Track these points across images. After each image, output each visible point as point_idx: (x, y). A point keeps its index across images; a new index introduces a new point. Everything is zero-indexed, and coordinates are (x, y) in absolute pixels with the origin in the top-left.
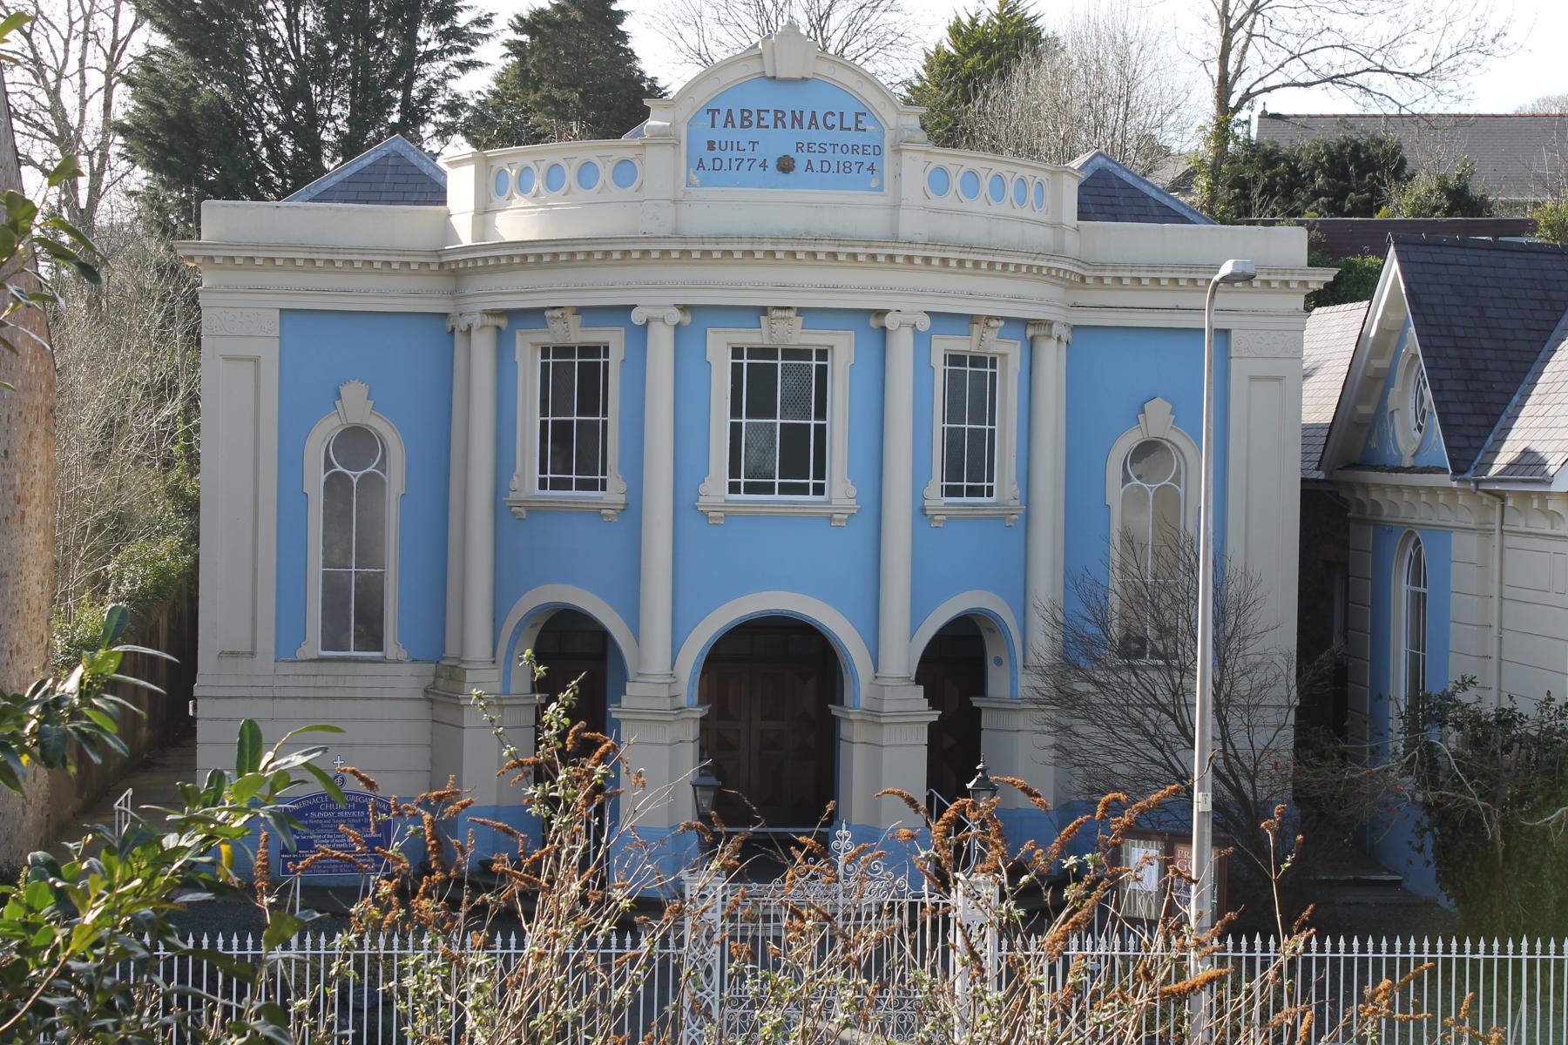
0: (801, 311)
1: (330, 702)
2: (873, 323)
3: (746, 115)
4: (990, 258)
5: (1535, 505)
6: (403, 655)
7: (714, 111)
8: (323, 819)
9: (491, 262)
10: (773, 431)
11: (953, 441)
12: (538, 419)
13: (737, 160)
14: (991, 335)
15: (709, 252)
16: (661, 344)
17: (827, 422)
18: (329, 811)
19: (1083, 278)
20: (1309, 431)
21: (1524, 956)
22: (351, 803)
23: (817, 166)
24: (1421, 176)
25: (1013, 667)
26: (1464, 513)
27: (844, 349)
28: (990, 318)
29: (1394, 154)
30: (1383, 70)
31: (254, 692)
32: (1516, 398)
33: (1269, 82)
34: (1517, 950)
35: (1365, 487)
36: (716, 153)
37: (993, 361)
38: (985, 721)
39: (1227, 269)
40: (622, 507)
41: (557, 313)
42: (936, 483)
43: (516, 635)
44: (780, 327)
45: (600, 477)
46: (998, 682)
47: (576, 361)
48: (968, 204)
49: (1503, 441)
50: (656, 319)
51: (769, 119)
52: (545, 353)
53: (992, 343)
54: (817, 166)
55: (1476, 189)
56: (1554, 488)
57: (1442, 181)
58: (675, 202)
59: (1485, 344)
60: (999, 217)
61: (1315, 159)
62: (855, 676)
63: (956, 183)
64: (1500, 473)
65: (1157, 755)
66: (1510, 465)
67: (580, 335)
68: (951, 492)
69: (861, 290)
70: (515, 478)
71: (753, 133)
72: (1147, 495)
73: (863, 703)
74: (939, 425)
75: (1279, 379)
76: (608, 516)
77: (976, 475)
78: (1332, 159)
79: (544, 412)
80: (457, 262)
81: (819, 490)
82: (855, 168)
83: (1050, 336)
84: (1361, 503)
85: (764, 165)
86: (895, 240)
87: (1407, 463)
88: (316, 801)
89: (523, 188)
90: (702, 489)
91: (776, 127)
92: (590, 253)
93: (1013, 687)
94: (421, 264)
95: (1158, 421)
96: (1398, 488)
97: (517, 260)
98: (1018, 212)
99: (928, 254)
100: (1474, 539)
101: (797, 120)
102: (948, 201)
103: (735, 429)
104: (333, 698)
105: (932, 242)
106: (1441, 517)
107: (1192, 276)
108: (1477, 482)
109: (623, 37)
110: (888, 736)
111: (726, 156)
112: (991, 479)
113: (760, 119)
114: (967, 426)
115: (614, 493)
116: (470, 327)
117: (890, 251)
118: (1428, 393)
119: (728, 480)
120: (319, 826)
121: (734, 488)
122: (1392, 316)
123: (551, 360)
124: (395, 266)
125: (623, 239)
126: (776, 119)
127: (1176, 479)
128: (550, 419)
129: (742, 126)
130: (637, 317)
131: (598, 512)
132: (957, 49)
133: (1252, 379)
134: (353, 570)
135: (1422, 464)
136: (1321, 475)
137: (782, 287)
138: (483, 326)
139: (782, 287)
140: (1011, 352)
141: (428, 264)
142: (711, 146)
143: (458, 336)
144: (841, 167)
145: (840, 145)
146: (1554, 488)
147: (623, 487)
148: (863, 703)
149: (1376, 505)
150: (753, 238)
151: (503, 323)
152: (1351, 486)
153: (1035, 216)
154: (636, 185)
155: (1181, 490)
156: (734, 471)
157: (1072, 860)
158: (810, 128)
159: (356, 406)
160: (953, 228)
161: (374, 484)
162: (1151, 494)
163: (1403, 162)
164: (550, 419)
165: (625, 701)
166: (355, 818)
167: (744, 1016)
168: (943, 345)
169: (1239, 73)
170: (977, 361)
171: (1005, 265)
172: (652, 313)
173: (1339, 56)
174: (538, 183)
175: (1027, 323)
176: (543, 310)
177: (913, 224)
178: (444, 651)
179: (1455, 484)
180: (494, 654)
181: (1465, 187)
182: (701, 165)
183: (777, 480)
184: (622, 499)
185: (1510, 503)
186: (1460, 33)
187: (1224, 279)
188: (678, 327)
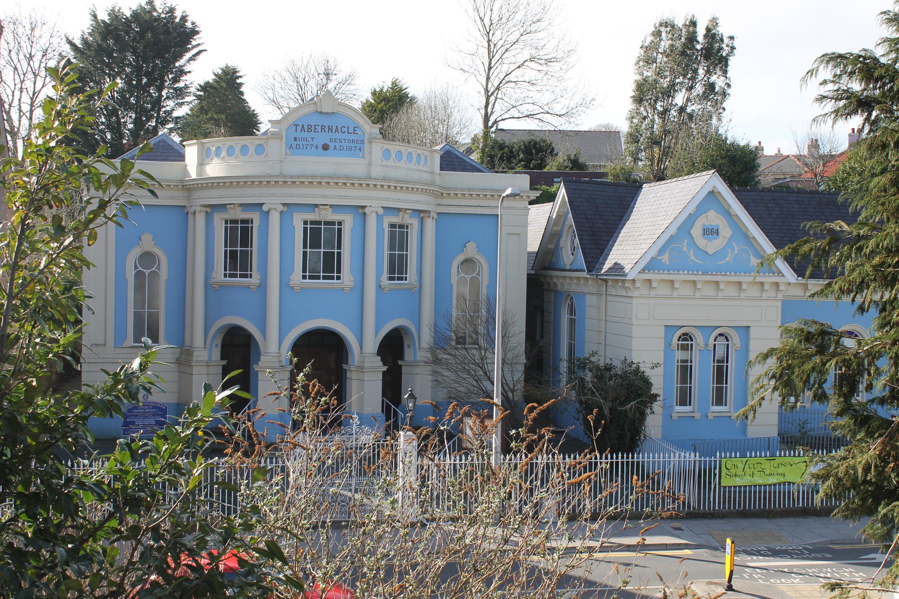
0: (331, 206)
2: (360, 211)
4: (407, 186)
5: (620, 284)
7: (296, 125)
9: (204, 185)
10: (320, 254)
11: (392, 258)
12: (223, 249)
14: (407, 216)
15: (295, 182)
16: (275, 219)
19: (442, 194)
20: (529, 253)
21: (620, 460)
24: (561, 154)
25: (415, 348)
26: (591, 287)
27: (349, 222)
28: (406, 209)
29: (550, 146)
30: (548, 113)
31: (106, 360)
32: (611, 243)
33: (504, 117)
34: (617, 458)
35: (551, 277)
36: (298, 142)
37: (407, 226)
38: (404, 370)
39: (509, 191)
41: (232, 206)
42: (386, 275)
44: (323, 212)
45: (249, 273)
46: (408, 354)
47: (239, 225)
48: (398, 164)
49: (606, 259)
50: (272, 209)
51: (319, 129)
52: (226, 222)
53: (407, 219)
54: (338, 148)
55: (581, 160)
56: (628, 278)
57: (569, 156)
58: (280, 161)
59: (599, 221)
60: (410, 169)
61: (519, 147)
62: (353, 352)
63: (393, 155)
64: (606, 272)
65: (475, 383)
66: (609, 268)
67: (240, 215)
68: (391, 279)
69: (356, 198)
71: (312, 134)
73: (356, 363)
74: (386, 252)
75: (518, 234)
77: (401, 272)
78: (526, 147)
79: (226, 246)
80: (190, 185)
81: (339, 278)
82: (353, 149)
83: (429, 217)
84: (549, 283)
85: (317, 147)
86: (370, 178)
87: (568, 268)
89: (218, 155)
92: (246, 182)
93: (415, 357)
94: (175, 186)
95: (471, 250)
96: (564, 277)
97: (215, 185)
98: (417, 167)
99: (382, 184)
100: (595, 297)
101: (330, 129)
102: (390, 163)
103: (305, 253)
105: (384, 179)
106: (582, 288)
107: (495, 194)
108: (597, 275)
109: (242, 93)
110: (366, 376)
111: (301, 143)
112: (406, 274)
113: (315, 129)
114: (397, 252)
115: (255, 280)
116: (195, 212)
117: (368, 183)
118: (577, 241)
120: (137, 415)
121: (304, 277)
122: (562, 210)
123: (229, 225)
124: (172, 187)
125: (259, 177)
126: (322, 129)
127: (478, 274)
128: (228, 249)
130: (265, 208)
131: (248, 287)
132: (375, 100)
133: (508, 234)
135: (575, 268)
136: (533, 272)
137: (325, 196)
138: (201, 211)
139: (325, 196)
140: (415, 223)
141: (177, 186)
142: (295, 139)
143: (190, 215)
146: (628, 278)
147: (259, 277)
148: (356, 363)
149: (555, 284)
150: (313, 177)
151: (209, 210)
152: (545, 277)
153: (424, 169)
154: (264, 155)
155: (480, 278)
156: (304, 270)
157: (514, 431)
159: (148, 243)
160: (393, 174)
161: (154, 275)
163: (553, 149)
164: (228, 249)
167: (324, 491)
168: (388, 220)
169: (492, 113)
170: (401, 226)
171: (413, 188)
172: (271, 206)
173: (531, 107)
174: (224, 153)
175: (420, 211)
176: (226, 204)
177: (376, 171)
178: (184, 343)
179: (588, 276)
181: (578, 159)
182: (291, 147)
183: (322, 274)
184: (258, 282)
185: (610, 283)
186: (577, 99)
187: (508, 196)
188: (281, 212)
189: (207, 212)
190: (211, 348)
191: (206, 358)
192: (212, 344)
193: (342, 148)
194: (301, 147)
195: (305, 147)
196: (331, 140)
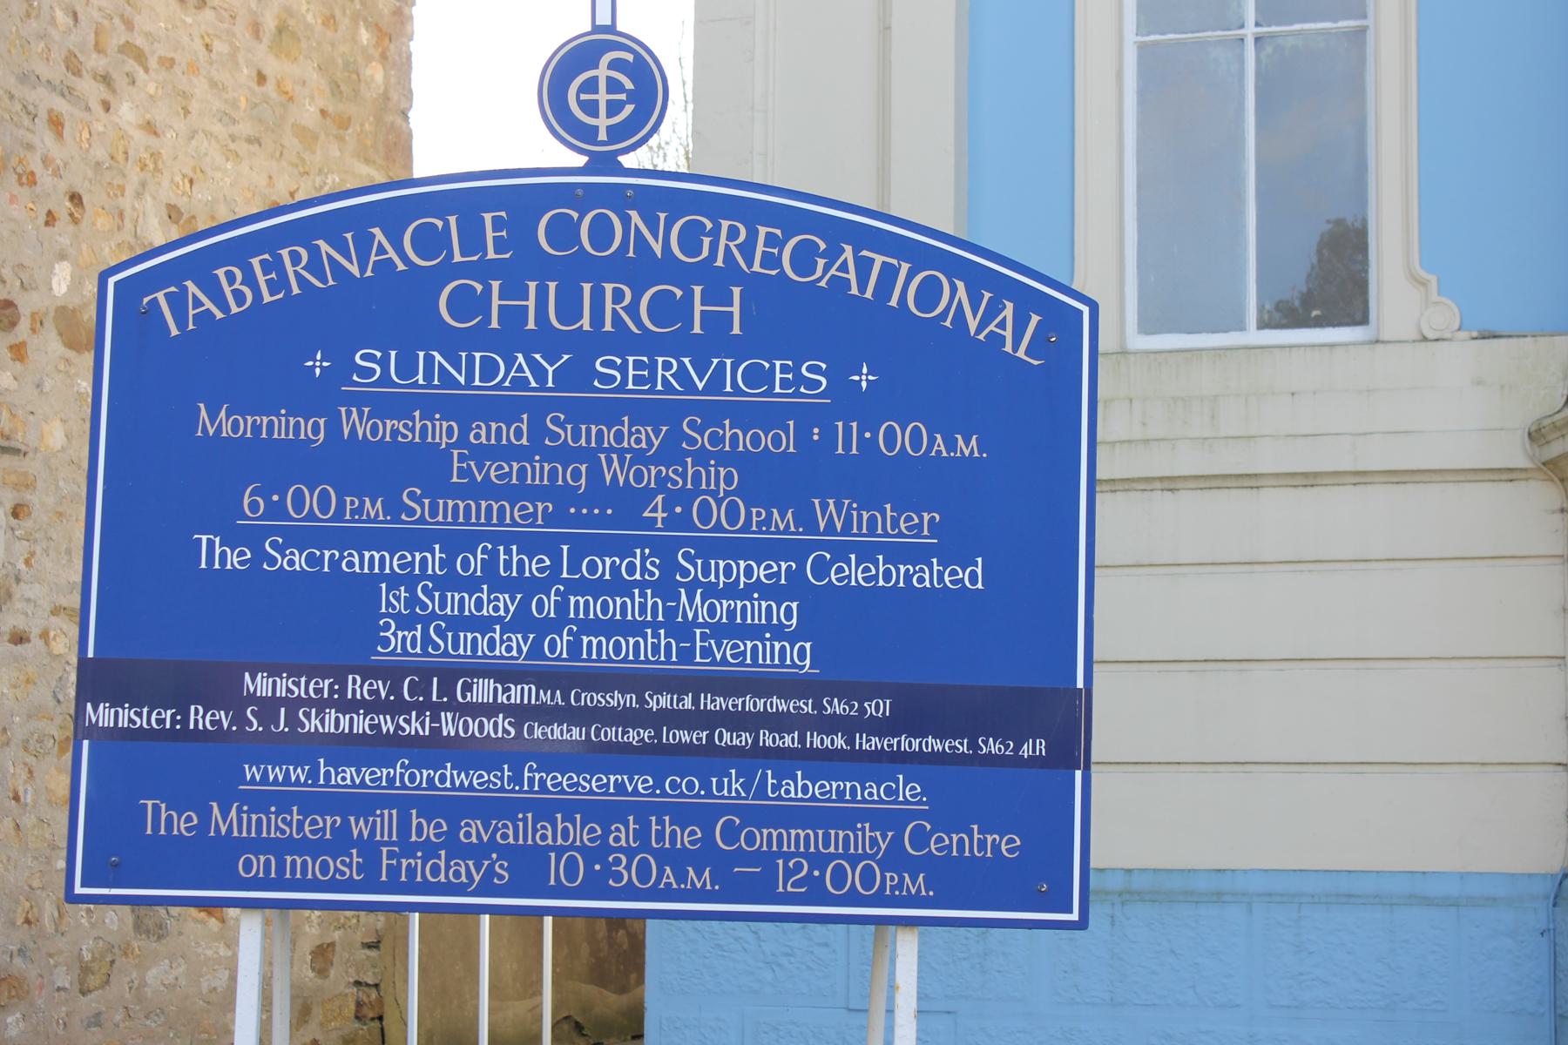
1: (1162, 502)
6: (1444, 317)
8: (466, 410)
18: (512, 337)
22: (717, 282)
88: (405, 254)
104: (1171, 483)
134: (1250, 30)
166: (746, 416)
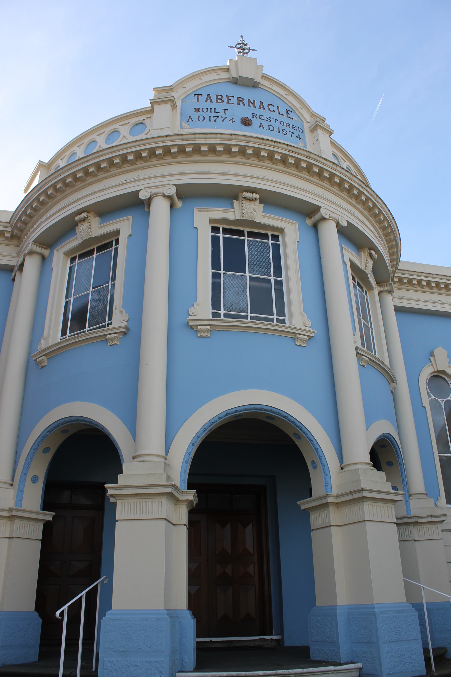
2: (309, 222)
3: (219, 98)
13: (214, 117)
17: (284, 279)
23: (266, 126)
36: (201, 113)
40: (124, 330)
43: (31, 457)
51: (235, 100)
54: (266, 126)
70: (43, 341)
71: (225, 105)
72: (440, 405)
76: (111, 339)
85: (232, 120)
90: (191, 311)
91: (239, 104)
93: (408, 508)
101: (252, 103)
111: (207, 115)
113: (228, 100)
119: (211, 311)
126: (239, 101)
129: (217, 102)
142: (197, 110)
144: (281, 131)
145: (279, 121)
156: (216, 304)
158: (260, 108)
162: (443, 405)
165: (122, 480)
180: (13, 479)
189: (43, 258)
190: (23, 482)
191: (11, 504)
192: (25, 473)
193: (271, 128)
194: (207, 118)
195: (213, 119)
196: (254, 115)
